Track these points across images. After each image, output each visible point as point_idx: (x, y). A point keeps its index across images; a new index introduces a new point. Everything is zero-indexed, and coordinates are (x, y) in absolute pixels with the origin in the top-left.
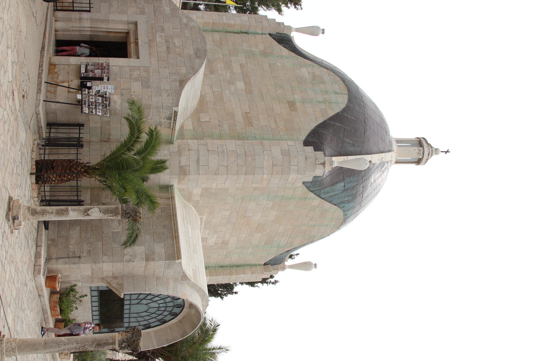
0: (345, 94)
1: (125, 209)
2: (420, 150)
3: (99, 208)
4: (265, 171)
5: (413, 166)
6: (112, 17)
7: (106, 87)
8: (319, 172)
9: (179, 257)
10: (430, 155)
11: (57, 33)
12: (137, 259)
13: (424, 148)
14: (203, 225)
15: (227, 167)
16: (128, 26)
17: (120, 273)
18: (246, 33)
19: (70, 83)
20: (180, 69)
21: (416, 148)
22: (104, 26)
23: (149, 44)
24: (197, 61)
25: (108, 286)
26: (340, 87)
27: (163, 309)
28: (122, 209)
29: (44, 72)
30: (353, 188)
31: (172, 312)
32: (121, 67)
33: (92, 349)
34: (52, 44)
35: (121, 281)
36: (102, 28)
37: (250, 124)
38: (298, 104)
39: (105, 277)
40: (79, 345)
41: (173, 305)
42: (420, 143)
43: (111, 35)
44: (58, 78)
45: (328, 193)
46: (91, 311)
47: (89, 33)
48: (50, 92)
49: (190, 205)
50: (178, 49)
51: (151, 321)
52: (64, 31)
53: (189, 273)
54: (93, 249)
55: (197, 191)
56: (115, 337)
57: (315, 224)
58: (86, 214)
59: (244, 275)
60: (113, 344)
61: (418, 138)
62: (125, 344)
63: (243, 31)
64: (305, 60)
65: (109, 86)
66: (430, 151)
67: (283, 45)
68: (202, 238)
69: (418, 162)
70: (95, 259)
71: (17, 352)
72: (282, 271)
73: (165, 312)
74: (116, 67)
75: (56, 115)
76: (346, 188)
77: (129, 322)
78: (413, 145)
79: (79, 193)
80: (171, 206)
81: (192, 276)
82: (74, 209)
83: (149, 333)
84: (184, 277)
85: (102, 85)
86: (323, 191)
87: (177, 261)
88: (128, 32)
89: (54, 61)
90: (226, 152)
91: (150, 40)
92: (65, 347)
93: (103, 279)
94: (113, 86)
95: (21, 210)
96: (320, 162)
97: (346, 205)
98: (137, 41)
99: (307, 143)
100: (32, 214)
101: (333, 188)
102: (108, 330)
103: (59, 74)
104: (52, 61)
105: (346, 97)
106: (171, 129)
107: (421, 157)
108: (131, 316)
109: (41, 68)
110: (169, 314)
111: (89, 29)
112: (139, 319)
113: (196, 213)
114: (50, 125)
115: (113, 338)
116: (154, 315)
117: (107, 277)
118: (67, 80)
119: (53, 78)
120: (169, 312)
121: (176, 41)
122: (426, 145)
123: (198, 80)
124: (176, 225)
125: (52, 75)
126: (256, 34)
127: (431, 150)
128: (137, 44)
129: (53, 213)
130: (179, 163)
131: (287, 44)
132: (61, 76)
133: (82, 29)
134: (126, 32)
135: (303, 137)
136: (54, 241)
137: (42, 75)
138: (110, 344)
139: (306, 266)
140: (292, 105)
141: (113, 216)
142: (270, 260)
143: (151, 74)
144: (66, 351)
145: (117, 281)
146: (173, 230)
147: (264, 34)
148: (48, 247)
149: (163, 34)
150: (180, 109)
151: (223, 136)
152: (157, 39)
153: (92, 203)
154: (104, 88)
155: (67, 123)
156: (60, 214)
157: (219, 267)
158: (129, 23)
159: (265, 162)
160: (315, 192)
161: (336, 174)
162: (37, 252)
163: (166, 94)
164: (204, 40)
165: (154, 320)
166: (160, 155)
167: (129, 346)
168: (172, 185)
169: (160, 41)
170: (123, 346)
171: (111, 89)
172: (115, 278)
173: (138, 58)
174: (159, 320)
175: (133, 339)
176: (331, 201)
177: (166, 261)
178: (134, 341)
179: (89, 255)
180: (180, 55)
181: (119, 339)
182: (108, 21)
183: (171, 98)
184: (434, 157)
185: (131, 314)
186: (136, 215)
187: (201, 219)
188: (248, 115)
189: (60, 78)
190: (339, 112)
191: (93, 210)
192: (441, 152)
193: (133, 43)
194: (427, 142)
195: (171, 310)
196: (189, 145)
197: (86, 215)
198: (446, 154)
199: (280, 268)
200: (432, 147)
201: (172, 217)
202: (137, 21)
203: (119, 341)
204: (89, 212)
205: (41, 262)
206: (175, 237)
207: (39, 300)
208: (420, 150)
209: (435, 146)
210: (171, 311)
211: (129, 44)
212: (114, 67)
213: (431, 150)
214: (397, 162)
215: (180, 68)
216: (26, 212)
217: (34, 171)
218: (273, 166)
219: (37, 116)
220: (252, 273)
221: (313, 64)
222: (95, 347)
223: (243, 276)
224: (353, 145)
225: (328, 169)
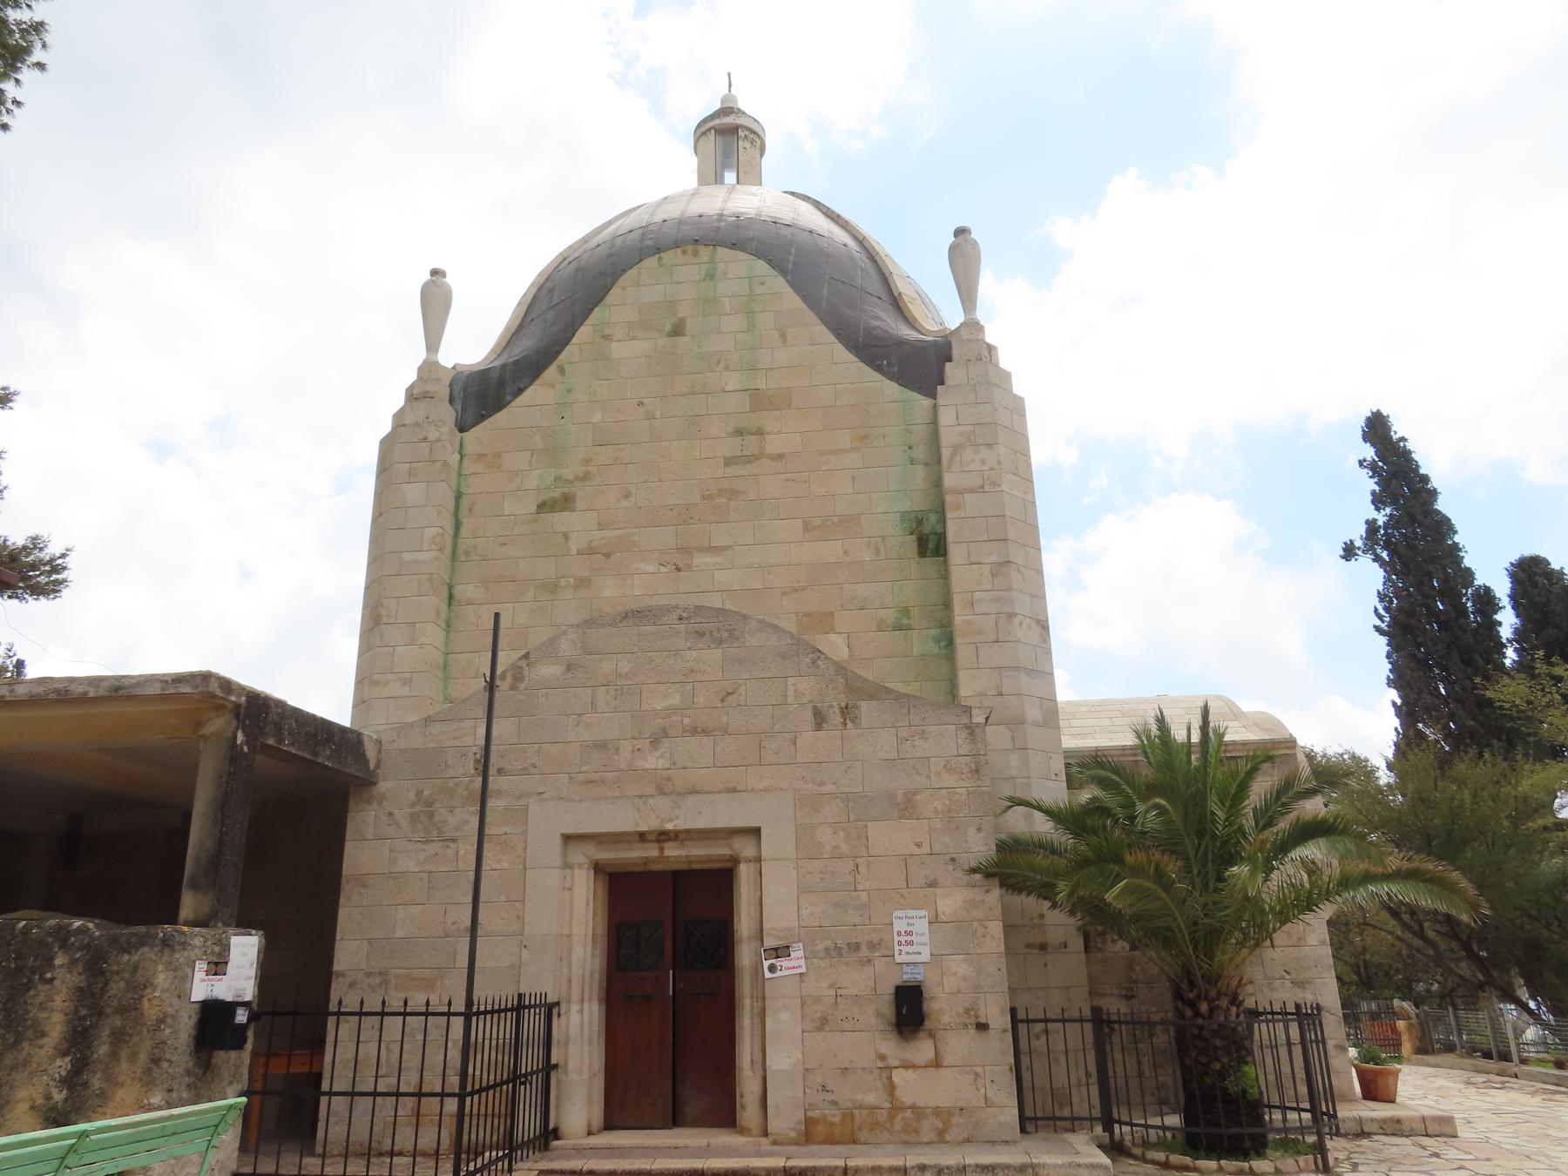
7: (903, 939)
16: (576, 866)
19: (893, 1062)
20: (798, 694)
34: (703, 1142)
44: (873, 1108)
50: (701, 700)
54: (1288, 973)
64: (574, 341)
65: (899, 925)
67: (508, 398)
70: (1319, 966)
79: (1050, 1015)
85: (897, 953)
88: (594, 868)
89: (791, 1126)
90: (997, 593)
91: (661, 791)
94: (896, 913)
98: (653, 837)
104: (793, 1134)
118: (880, 1075)
119: (875, 1126)
125: (860, 1129)
128: (663, 837)
132: (859, 1097)
134: (595, 873)
137: (948, 1168)
143: (830, 788)
151: (901, 601)
152: (652, 767)
153: (1134, 977)
162: (1381, 1131)
163: (919, 742)
164: (650, 611)
166: (1026, 777)
169: (662, 757)
171: (911, 921)
173: (756, 832)
180: (729, 694)
188: (815, 524)
189: (871, 1099)
190: (788, 282)
192: (730, 91)
193: (662, 849)
202: (562, 834)
208: (746, 136)
212: (804, 912)
215: (791, 692)
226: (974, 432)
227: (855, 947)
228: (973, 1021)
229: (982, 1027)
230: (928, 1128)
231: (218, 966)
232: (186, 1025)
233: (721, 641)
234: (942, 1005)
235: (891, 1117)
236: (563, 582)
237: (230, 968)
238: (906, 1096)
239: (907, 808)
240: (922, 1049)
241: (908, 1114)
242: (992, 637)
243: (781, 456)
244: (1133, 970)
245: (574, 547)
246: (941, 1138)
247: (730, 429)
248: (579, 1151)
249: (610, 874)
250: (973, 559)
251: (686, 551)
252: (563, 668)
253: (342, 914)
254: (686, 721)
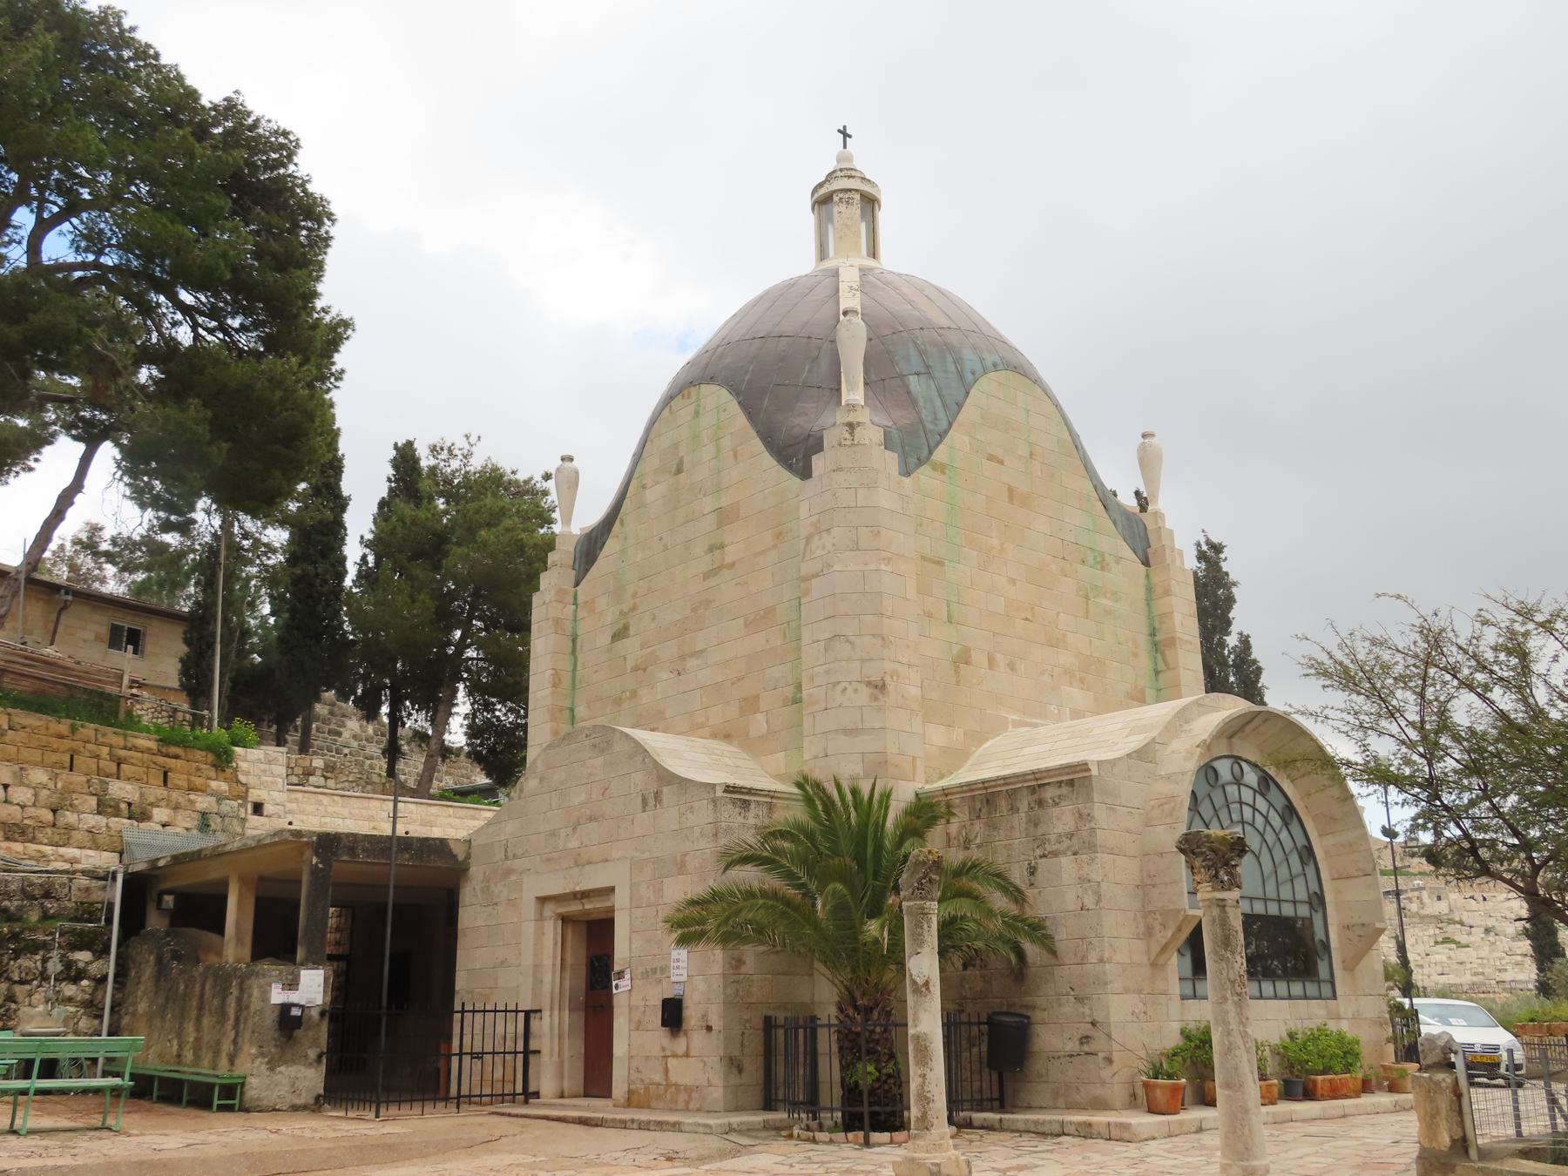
0: (699, 393)
1: (911, 890)
2: (841, 199)
3: (910, 957)
4: (872, 566)
5: (882, 216)
6: (528, 960)
7: (675, 964)
8: (871, 435)
9: (1083, 767)
10: (853, 173)
11: (566, 1094)
12: (1093, 876)
13: (835, 191)
14: (1034, 721)
15: (863, 661)
17: (1135, 919)
18: (574, 641)
19: (668, 1053)
21: (836, 209)
22: (548, 978)
23: (583, 866)
24: (617, 747)
25: (1176, 948)
26: (684, 410)
27: (1247, 812)
28: (910, 900)
29: (636, 1117)
30: (921, 353)
31: (1256, 787)
32: (633, 931)
33: (1240, 963)
35: (1157, 916)
36: (553, 981)
37: (770, 612)
38: (725, 502)
39: (1149, 959)
40: (1229, 994)
41: (1235, 787)
42: (823, 201)
43: (569, 961)
45: (935, 413)
46: (1261, 1001)
47: (567, 1013)
48: (687, 1103)
49: (976, 754)
50: (594, 796)
51: (1288, 844)
52: (561, 1076)
53: (1136, 742)
55: (938, 736)
56: (1204, 900)
58: (924, 989)
59: (1176, 614)
60: (1224, 906)
61: (813, 209)
62: (1221, 873)
63: (569, 650)
66: (842, 174)
68: (1071, 720)
69: (870, 202)
71: (1255, 1163)
72: (1163, 521)
73: (1257, 807)
74: (633, 941)
75: (741, 1085)
76: (922, 370)
77: (1295, 902)
78: (830, 219)
80: (964, 795)
81: (1141, 737)
82: (914, 1021)
83: (1326, 852)
84: (1144, 754)
86: (930, 426)
87: (1094, 771)
92: (1235, 1033)
93: (1156, 965)
95: (917, 1155)
96: (848, 436)
97: (968, 366)
98: (579, 896)
99: (805, 473)
100: (927, 1129)
101: (921, 403)
102: (1322, 960)
103: (647, 1081)
105: (704, 387)
106: (774, 801)
107: (857, 197)
108: (1275, 896)
109: (629, 1124)
110: (1263, 795)
111: (556, 1013)
112: (1283, 872)
113: (1001, 737)
114: (768, 1105)
115: (1209, 907)
116: (1270, 837)
117: (1148, 952)
119: (659, 1097)
120: (1258, 796)
121: (576, 801)
122: (826, 186)
123: (661, 745)
124: (1009, 781)
126: (575, 616)
127: (839, 174)
128: (585, 895)
129: (925, 1075)
131: (596, 543)
133: (556, 1031)
135: (793, 481)
136: (1058, 1093)
138: (1225, 912)
139: (1148, 460)
140: (725, 517)
141: (929, 921)
142: (1135, 553)
143: (647, 855)
144: (1246, 1032)
145: (1158, 927)
146: (1020, 785)
147: (575, 598)
148: (1071, 1107)
149: (563, 833)
150: (719, 777)
154: (678, 968)
155: (762, 1058)
156: (925, 1057)
157: (1157, 680)
158: (540, 918)
159: (850, 569)
160: (932, 444)
161: (885, 396)
162: (1076, 1133)
163: (690, 815)
165: (1284, 835)
167: (1226, 864)
168: (917, 795)
170: (1226, 878)
172: (1149, 932)
173: (612, 889)
174: (1286, 824)
175: (1208, 853)
176: (957, 404)
177: (1095, 800)
178: (1213, 850)
179: (1087, 998)
180: (606, 789)
181: (1210, 889)
182: (537, 967)
183: (696, 804)
184: (858, 164)
185: (1268, 897)
186: (924, 863)
187: (1017, 724)
190: (739, 403)
191: (914, 972)
192: (845, 147)
194: (821, 185)
195: (1252, 792)
196: (816, 757)
197: (928, 989)
198: (850, 137)
199: (1157, 523)
200: (834, 172)
201: (989, 791)
203: (1214, 889)
204: (920, 981)
205: (1099, 1124)
206: (1037, 779)
207: (1212, 1132)
208: (841, 199)
210: (1255, 791)
211: (588, 914)
213: (839, 174)
214: (873, 253)
216: (921, 1142)
217: (861, 1134)
218: (858, 549)
219: (735, 1131)
220: (1167, 592)
221: (636, 475)
222: (1233, 953)
223: (1177, 618)
224: (816, 360)
225: (863, 416)
226: (819, 520)
227: (654, 970)
228: (704, 1024)
229: (709, 1028)
230: (682, 1097)
231: (292, 985)
232: (270, 1019)
233: (603, 751)
234: (691, 1014)
235: (666, 1091)
236: (624, 697)
237: (300, 987)
238: (674, 1077)
239: (681, 867)
240: (680, 1045)
241: (673, 1089)
242: (823, 707)
243: (732, 565)
244: (963, 987)
245: (630, 664)
246: (687, 1109)
247: (706, 547)
248: (550, 1106)
249: (589, 922)
250: (815, 638)
251: (683, 658)
252: (538, 780)
253: (458, 952)
254: (588, 812)
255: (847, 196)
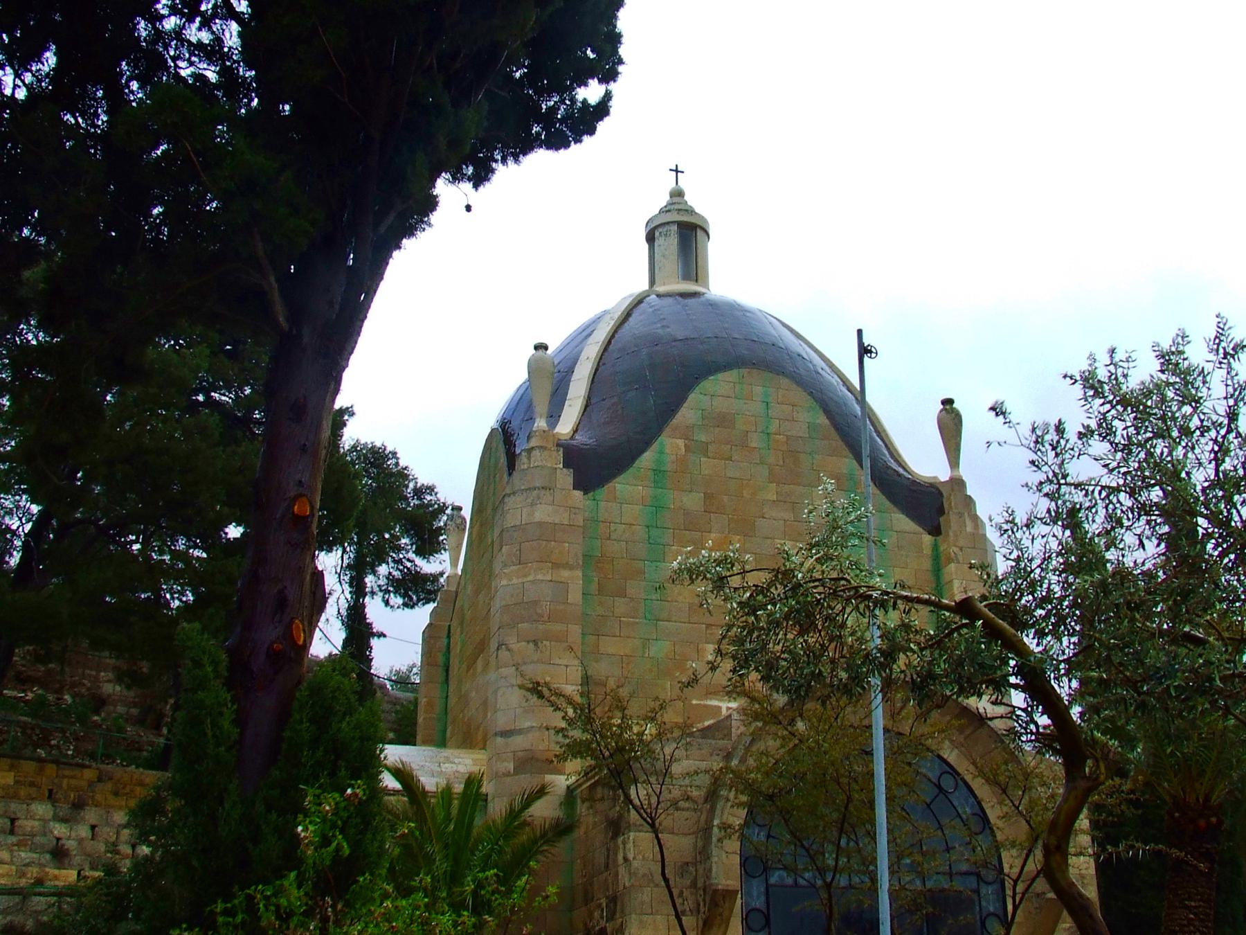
2: (660, 233)
57: (762, 432)
107: (675, 227)
130: (508, 774)
209: (664, 199)
255: (665, 229)
